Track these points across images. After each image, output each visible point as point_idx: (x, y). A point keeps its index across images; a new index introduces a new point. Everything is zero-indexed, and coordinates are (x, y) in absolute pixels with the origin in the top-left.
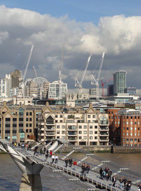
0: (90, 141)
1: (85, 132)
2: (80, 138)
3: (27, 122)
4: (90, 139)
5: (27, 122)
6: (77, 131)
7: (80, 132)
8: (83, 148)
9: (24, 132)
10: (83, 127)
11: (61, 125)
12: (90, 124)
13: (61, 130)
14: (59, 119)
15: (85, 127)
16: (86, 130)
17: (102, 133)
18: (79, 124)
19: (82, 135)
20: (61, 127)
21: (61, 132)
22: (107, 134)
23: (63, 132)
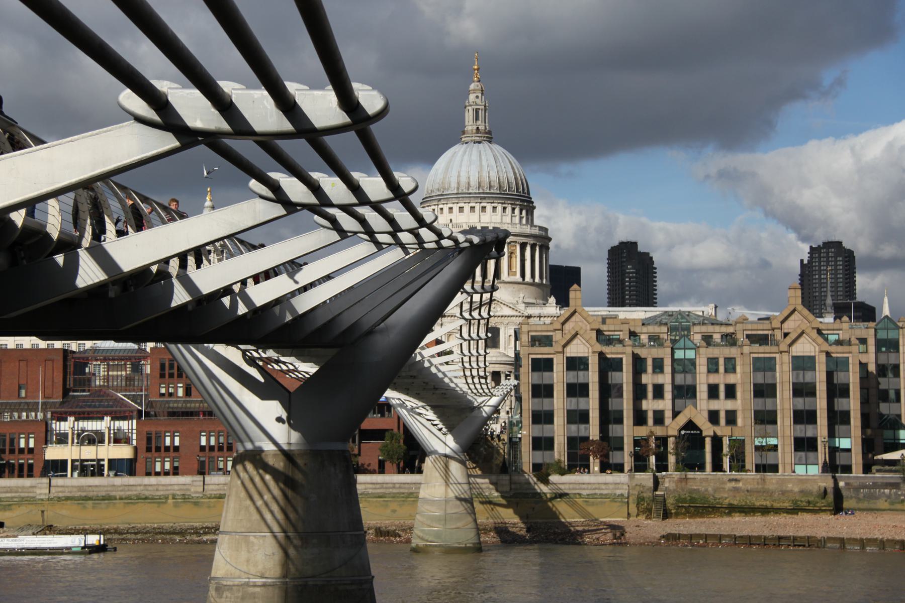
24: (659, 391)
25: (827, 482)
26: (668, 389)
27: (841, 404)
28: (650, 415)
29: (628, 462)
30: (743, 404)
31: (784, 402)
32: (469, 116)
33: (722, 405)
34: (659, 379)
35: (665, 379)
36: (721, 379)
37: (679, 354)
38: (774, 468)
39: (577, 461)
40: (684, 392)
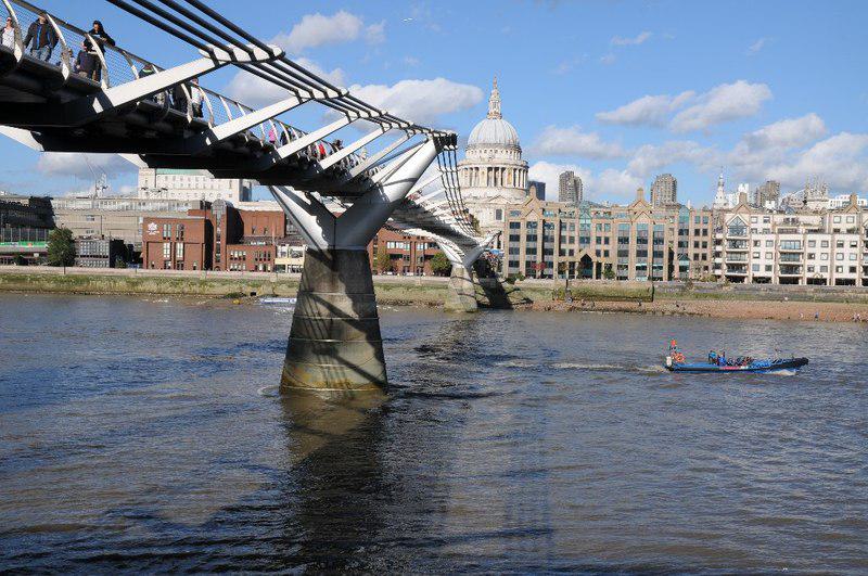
1: (825, 257)
3: (697, 239)
5: (697, 239)
7: (811, 256)
8: (816, 291)
9: (688, 259)
11: (763, 238)
12: (838, 237)
13: (762, 249)
14: (761, 226)
15: (825, 244)
16: (828, 250)
19: (817, 263)
20: (763, 243)
21: (762, 256)
24: (572, 240)
25: (649, 285)
26: (577, 239)
27: (659, 248)
28: (567, 252)
29: (555, 273)
30: (613, 247)
31: (633, 247)
32: (491, 104)
33: (602, 247)
34: (573, 234)
35: (575, 234)
36: (603, 235)
37: (583, 222)
38: (626, 278)
39: (531, 272)
40: (585, 240)
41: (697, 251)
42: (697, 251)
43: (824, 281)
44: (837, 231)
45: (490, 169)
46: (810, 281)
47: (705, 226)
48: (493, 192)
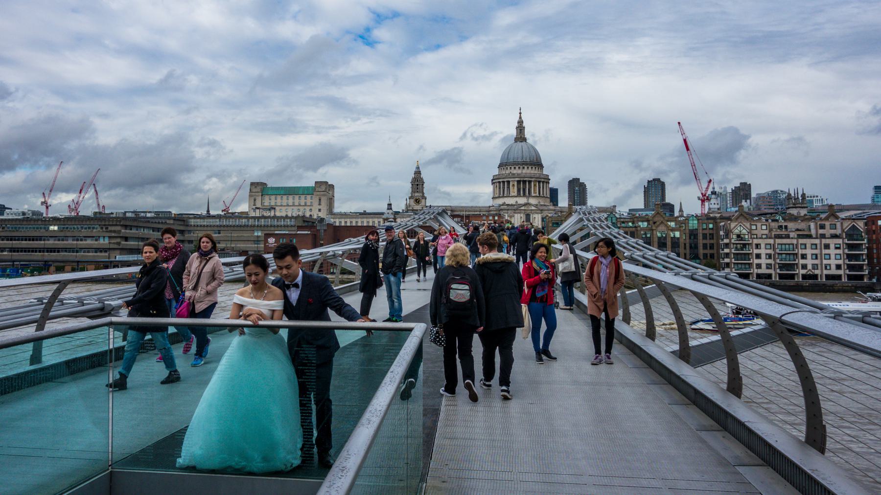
0: (825, 272)
2: (804, 267)
3: (705, 242)
4: (826, 268)
5: (705, 242)
6: (796, 254)
7: (804, 257)
10: (808, 246)
12: (824, 241)
17: (850, 257)
18: (801, 241)
19: (809, 262)
20: (763, 246)
21: (763, 256)
22: (864, 260)
23: (769, 256)
41: (706, 251)
42: (706, 251)
43: (815, 277)
44: (823, 236)
45: (519, 182)
46: (805, 277)
47: (711, 232)
48: (522, 200)
